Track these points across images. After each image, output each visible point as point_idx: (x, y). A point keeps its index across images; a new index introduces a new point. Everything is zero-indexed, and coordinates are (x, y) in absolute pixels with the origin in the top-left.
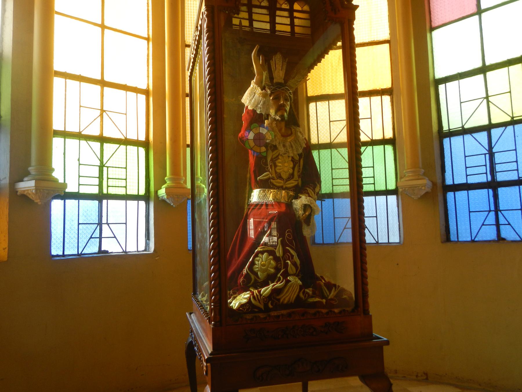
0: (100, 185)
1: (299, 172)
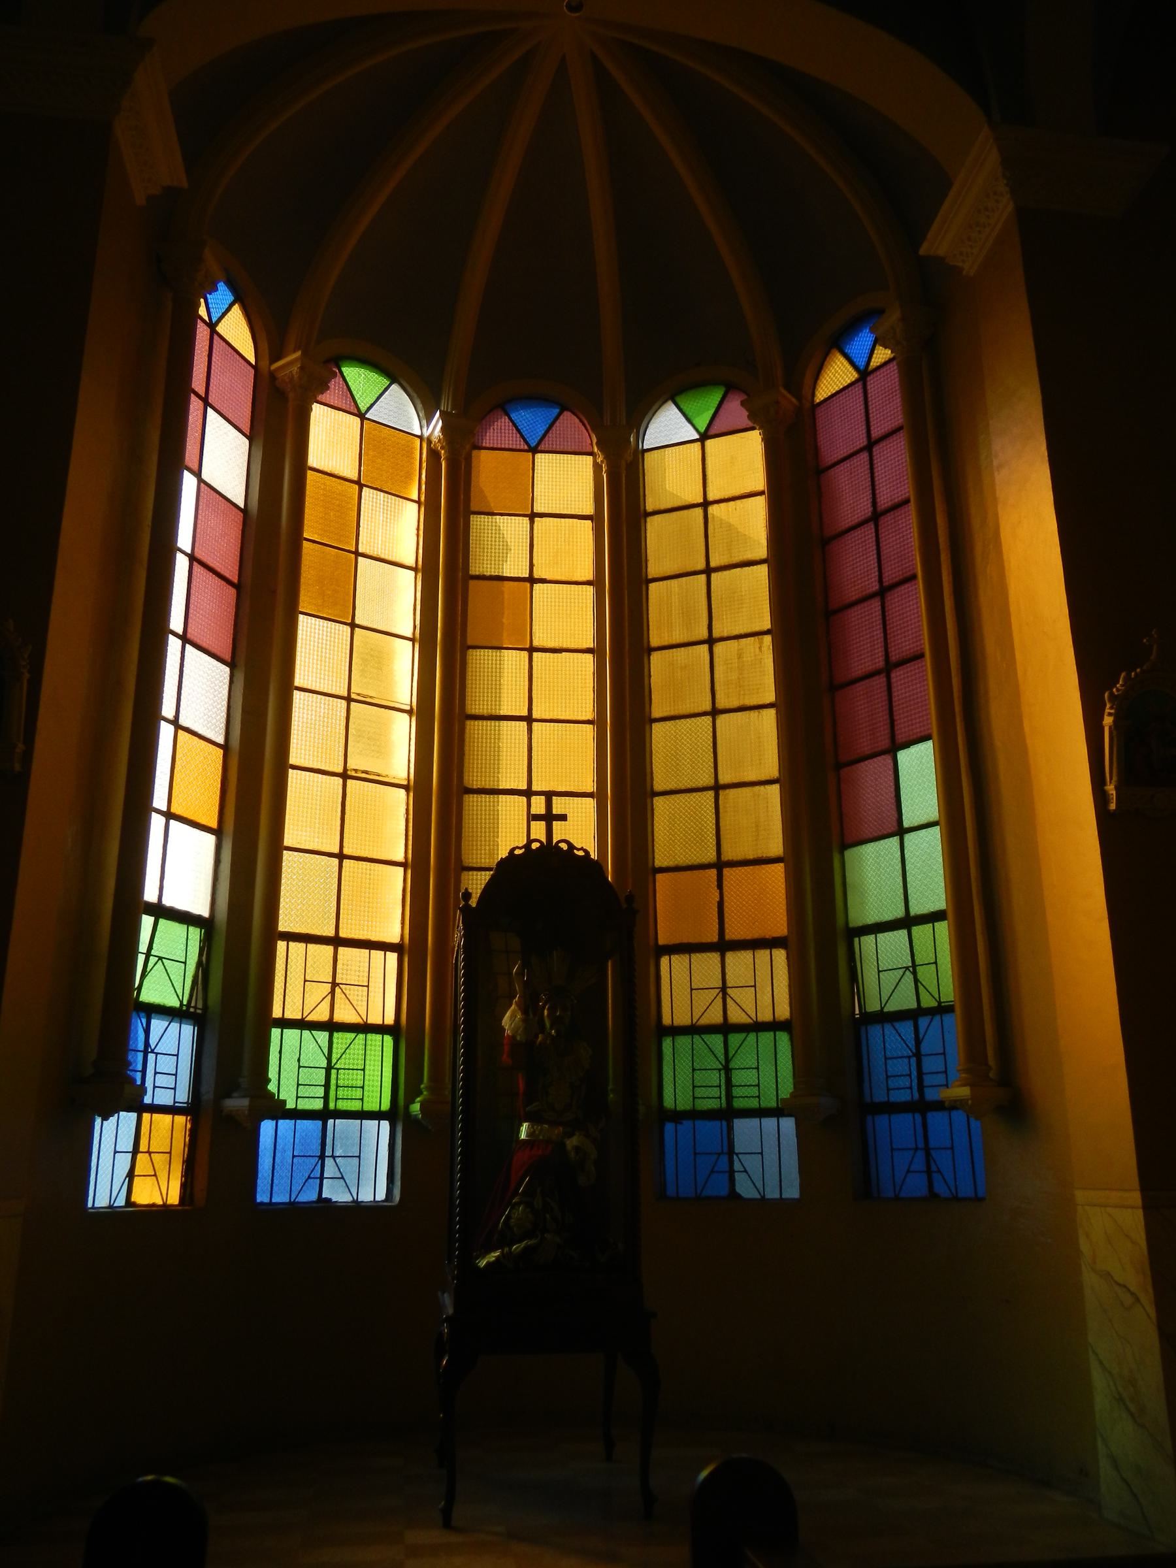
0: (326, 1098)
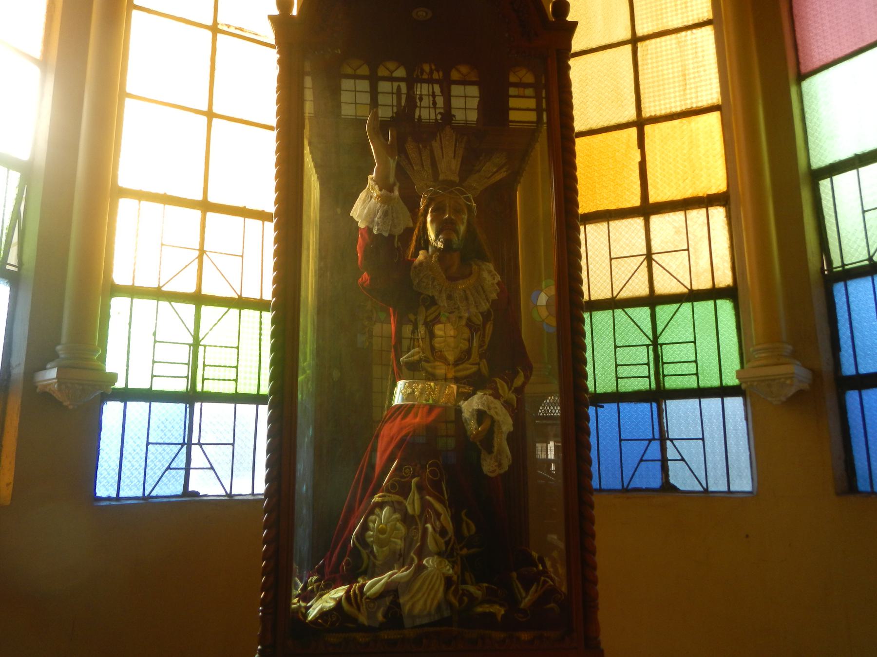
1: (481, 346)
